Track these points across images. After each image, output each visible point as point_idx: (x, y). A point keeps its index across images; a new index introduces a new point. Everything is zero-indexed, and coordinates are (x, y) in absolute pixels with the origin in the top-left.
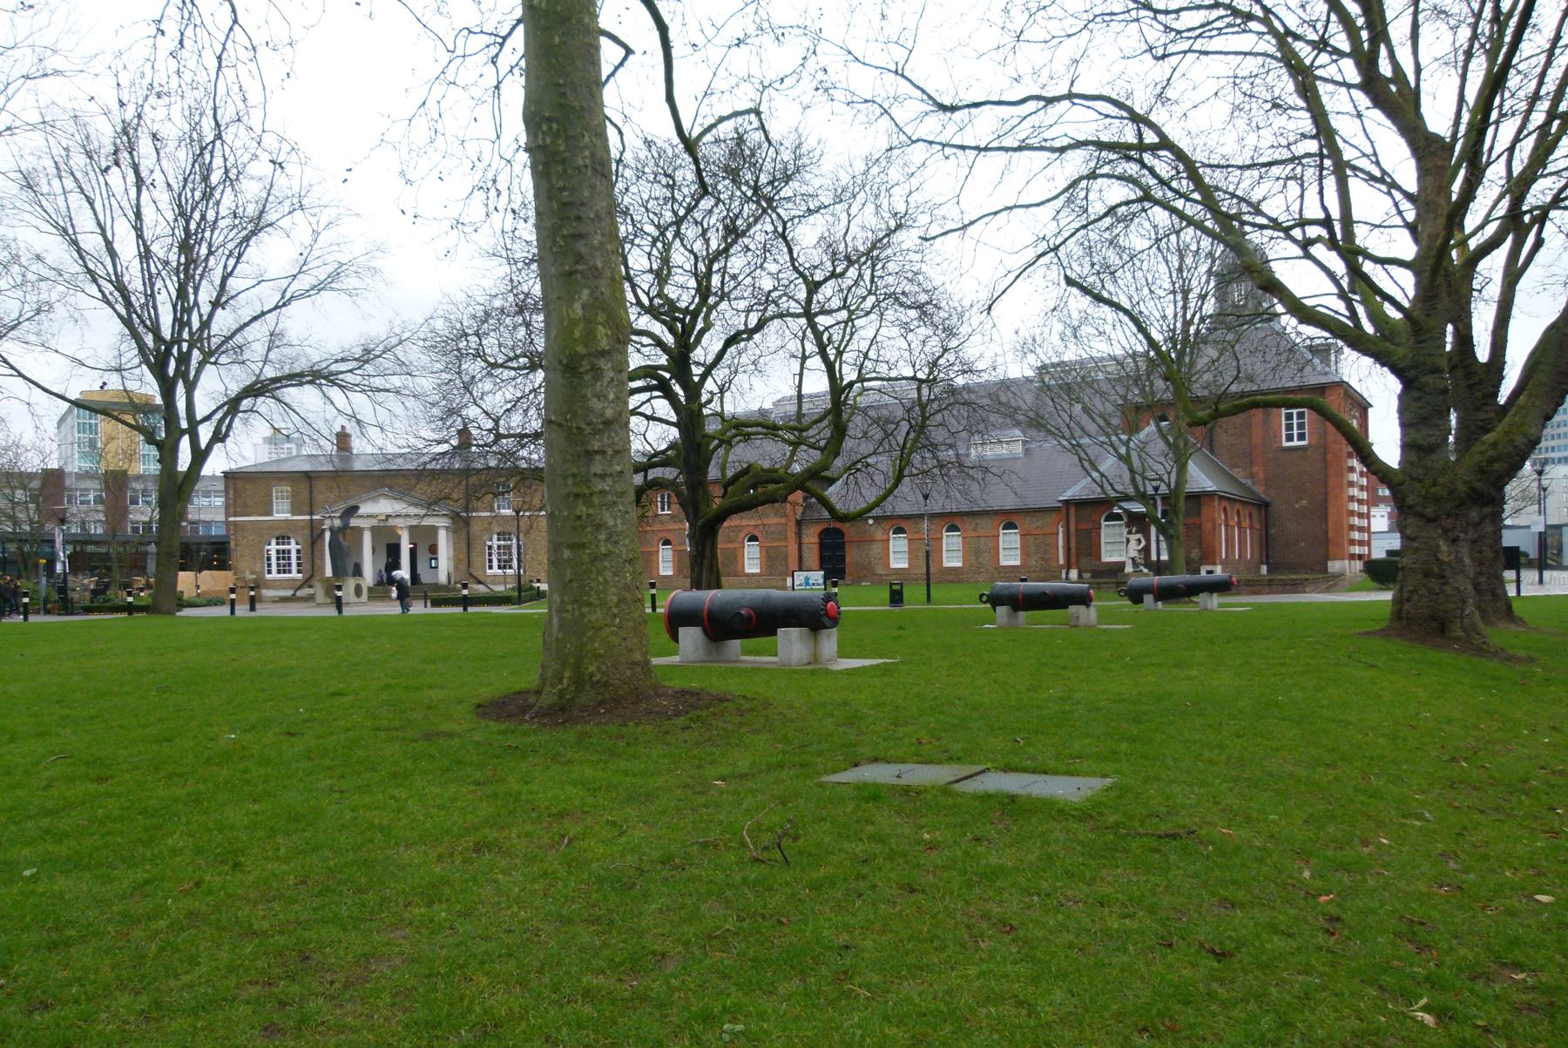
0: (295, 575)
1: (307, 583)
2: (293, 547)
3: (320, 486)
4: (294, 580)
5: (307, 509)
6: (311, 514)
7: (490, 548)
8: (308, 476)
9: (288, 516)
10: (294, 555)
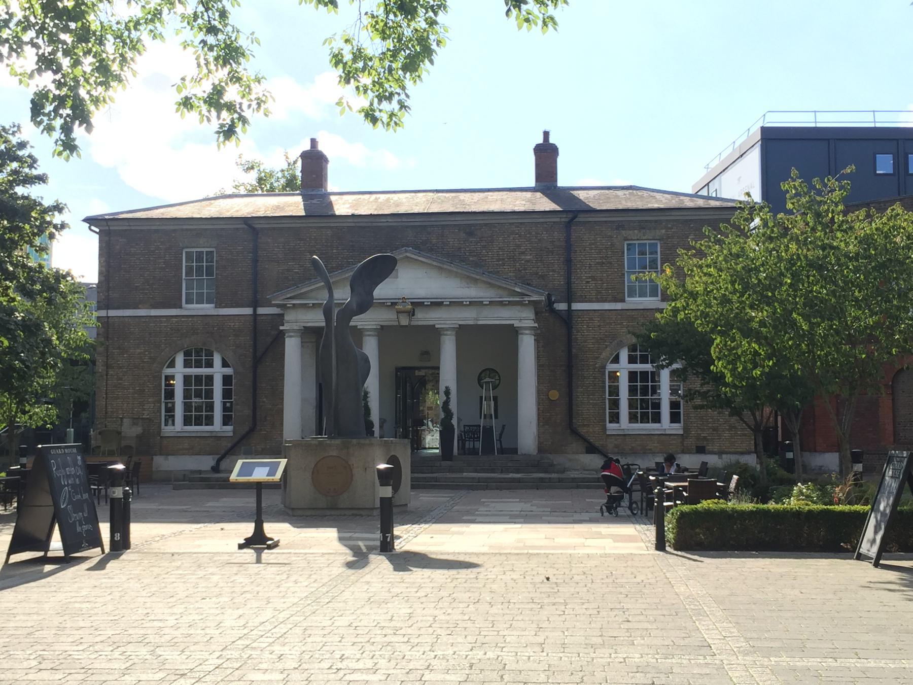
2: (218, 371)
4: (217, 438)
6: (255, 304)
7: (614, 377)
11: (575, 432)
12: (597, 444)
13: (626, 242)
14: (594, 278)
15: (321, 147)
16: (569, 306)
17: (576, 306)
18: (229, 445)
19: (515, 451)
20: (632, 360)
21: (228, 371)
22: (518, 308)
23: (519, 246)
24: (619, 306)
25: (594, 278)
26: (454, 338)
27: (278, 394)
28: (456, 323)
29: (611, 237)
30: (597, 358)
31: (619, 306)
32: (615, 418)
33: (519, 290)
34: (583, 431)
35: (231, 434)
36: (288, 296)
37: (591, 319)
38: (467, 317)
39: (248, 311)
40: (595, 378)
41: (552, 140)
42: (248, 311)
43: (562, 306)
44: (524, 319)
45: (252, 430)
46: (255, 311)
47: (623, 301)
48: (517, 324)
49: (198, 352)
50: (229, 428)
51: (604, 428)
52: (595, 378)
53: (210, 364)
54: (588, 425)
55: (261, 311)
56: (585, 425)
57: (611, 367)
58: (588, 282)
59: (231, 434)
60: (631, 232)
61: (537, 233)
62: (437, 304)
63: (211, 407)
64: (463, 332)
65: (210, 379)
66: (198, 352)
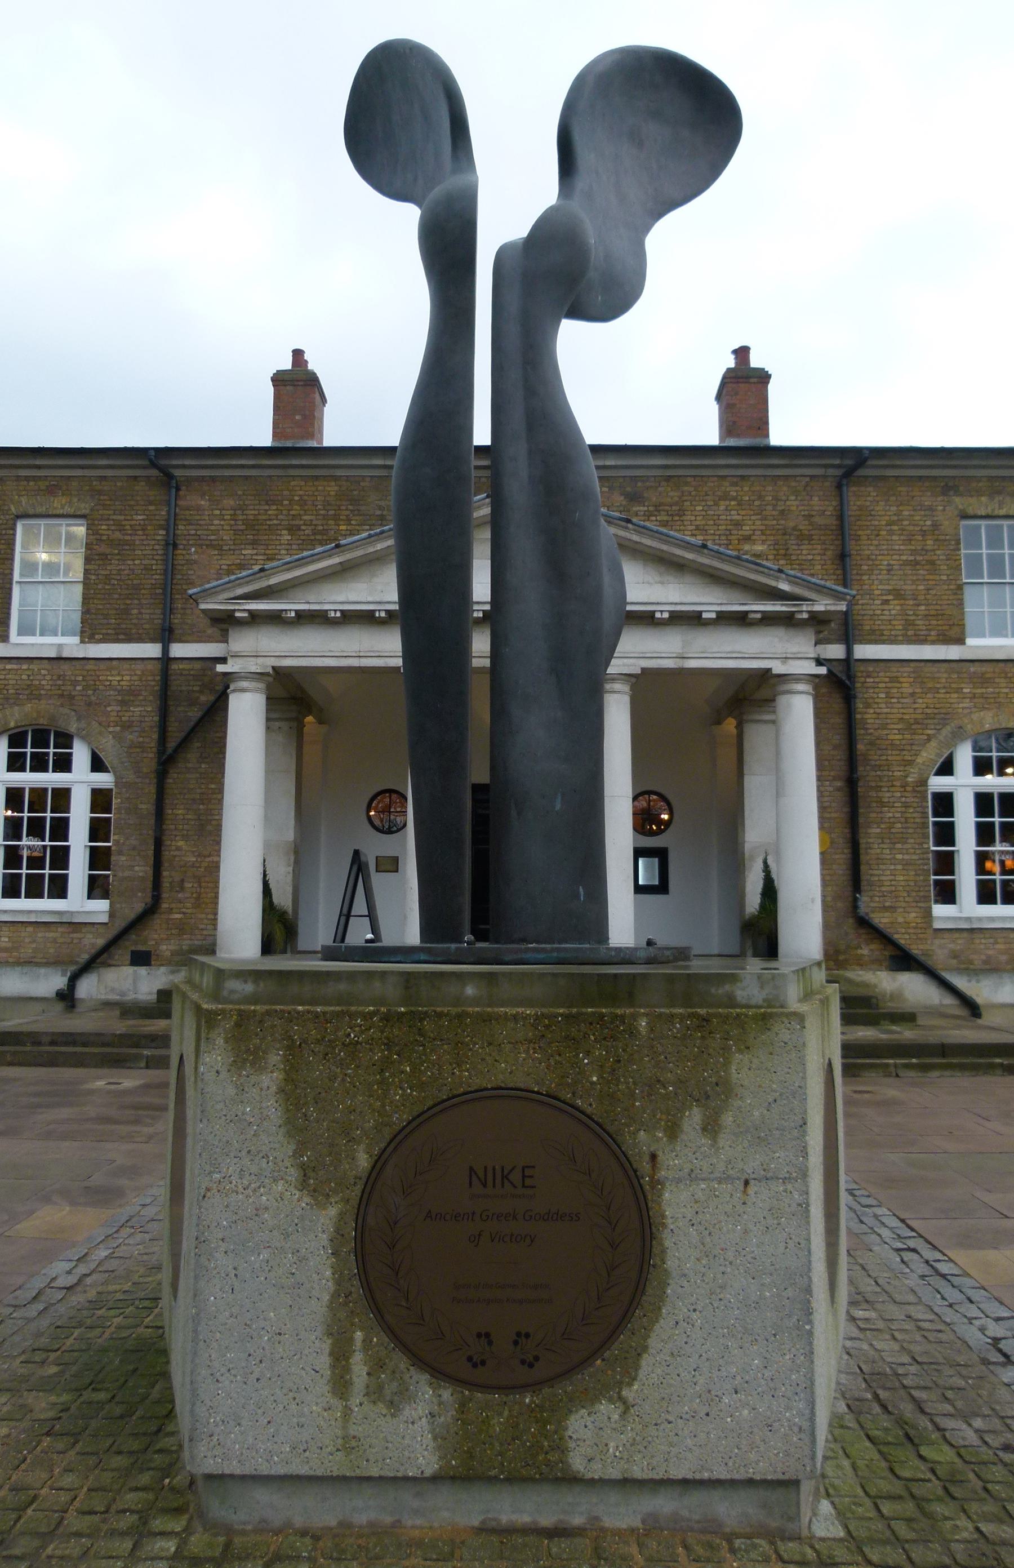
0: (78, 902)
1: (123, 943)
2: (81, 780)
3: (208, 511)
4: (74, 926)
5: (151, 615)
6: (167, 635)
7: (944, 803)
8: (163, 470)
9: (71, 645)
10: (80, 816)
13: (964, 522)
14: (898, 594)
15: (313, 365)
16: (849, 651)
17: (864, 651)
18: (101, 942)
20: (981, 767)
21: (104, 780)
23: (738, 524)
24: (952, 652)
25: (898, 594)
26: (626, 699)
27: (209, 830)
29: (931, 509)
30: (911, 763)
31: (952, 652)
32: (947, 893)
33: (784, 586)
34: (881, 920)
35: (104, 919)
36: (240, 591)
37: (894, 679)
39: (152, 650)
40: (906, 805)
41: (756, 361)
42: (152, 650)
44: (793, 655)
45: (151, 911)
46: (165, 651)
47: (960, 641)
48: (778, 668)
49: (41, 738)
50: (101, 906)
51: (928, 912)
52: (906, 805)
53: (64, 764)
54: (892, 909)
55: (179, 650)
56: (885, 909)
57: (939, 783)
58: (886, 602)
59: (104, 919)
60: (973, 500)
61: (776, 499)
63: (61, 857)
65: (62, 797)
66: (41, 738)
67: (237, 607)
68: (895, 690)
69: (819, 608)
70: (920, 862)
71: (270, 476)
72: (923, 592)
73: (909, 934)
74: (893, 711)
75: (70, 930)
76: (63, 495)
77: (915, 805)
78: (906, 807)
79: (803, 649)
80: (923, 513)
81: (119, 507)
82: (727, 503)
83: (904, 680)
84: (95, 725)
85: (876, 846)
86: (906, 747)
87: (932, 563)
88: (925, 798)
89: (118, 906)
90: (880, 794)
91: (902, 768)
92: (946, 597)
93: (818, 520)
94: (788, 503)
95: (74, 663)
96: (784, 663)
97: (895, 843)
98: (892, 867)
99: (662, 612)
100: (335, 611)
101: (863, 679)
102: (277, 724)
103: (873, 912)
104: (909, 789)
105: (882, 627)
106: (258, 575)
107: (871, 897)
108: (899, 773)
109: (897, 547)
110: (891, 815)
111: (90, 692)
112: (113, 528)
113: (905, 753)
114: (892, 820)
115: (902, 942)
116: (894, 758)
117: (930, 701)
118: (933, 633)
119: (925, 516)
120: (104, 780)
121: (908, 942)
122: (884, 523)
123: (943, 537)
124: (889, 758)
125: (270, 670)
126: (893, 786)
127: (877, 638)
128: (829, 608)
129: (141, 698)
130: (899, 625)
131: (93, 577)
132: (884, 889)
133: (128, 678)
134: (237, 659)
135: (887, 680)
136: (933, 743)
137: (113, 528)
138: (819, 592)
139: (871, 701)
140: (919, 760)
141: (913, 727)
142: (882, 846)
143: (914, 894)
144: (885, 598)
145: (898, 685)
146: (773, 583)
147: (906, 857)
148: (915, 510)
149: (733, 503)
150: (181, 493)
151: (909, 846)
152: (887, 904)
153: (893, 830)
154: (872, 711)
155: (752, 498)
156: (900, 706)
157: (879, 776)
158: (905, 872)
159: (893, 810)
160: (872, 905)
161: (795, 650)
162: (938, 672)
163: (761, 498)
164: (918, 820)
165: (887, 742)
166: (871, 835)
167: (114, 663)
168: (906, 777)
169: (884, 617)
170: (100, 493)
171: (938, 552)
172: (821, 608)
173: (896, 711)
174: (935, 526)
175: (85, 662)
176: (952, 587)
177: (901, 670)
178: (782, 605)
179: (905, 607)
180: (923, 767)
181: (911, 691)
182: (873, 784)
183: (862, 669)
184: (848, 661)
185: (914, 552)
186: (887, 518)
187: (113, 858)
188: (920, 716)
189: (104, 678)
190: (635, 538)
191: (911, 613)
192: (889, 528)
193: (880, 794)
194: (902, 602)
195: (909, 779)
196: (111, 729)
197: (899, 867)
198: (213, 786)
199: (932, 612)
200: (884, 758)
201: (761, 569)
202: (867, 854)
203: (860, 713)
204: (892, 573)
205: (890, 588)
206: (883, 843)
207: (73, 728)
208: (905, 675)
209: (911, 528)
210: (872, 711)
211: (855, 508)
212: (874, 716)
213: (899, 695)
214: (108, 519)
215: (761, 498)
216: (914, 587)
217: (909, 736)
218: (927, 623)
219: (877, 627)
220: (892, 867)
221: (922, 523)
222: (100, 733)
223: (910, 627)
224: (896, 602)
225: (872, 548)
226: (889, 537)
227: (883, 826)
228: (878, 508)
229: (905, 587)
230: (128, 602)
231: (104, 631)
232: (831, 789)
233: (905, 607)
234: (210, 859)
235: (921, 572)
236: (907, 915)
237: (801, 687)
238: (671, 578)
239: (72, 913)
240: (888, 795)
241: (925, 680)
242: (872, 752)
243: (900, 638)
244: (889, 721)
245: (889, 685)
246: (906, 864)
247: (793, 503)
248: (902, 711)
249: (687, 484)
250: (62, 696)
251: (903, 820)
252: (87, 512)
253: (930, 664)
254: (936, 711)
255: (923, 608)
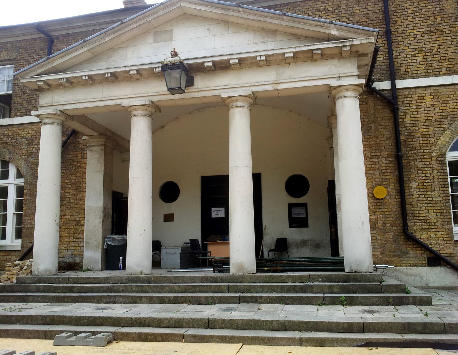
11: (410, 238)
12: (443, 253)
14: (421, 50)
16: (393, 84)
17: (401, 84)
19: (339, 264)
21: (21, 181)
22: (335, 62)
25: (421, 50)
28: (248, 91)
33: (334, 32)
34: (421, 236)
35: (19, 248)
38: (263, 81)
43: (383, 85)
48: (334, 83)
50: (19, 241)
51: (450, 232)
58: (414, 55)
59: (19, 248)
61: (347, 7)
62: (221, 66)
64: (256, 102)
67: (37, 80)
68: (422, 104)
69: (356, 42)
70: (444, 201)
71: (93, 30)
72: (436, 47)
73: (439, 244)
74: (422, 115)
75: (6, 254)
76: (5, 51)
77: (439, 168)
78: (433, 170)
79: (350, 70)
80: (434, 4)
81: (28, 54)
82: (320, 13)
83: (428, 97)
84: (16, 156)
85: (416, 193)
86: (431, 136)
87: (441, 31)
88: (444, 164)
89: (25, 242)
90: (416, 163)
91: (429, 148)
92: (451, 49)
93: (372, 15)
94: (354, 9)
95: (9, 127)
96: (338, 80)
97: (427, 191)
98: (426, 205)
99: (261, 56)
100: (85, 76)
101: (402, 100)
102: (95, 148)
103: (415, 232)
104: (434, 159)
105: (412, 69)
106: (47, 62)
107: (414, 223)
108: (427, 151)
109: (419, 25)
110: (424, 175)
111: (15, 140)
112: (25, 63)
113: (430, 139)
114: (424, 178)
115: (435, 249)
116: (424, 142)
117: (444, 108)
118: (443, 70)
119: (435, 5)
120: (21, 181)
121: (439, 249)
122: (410, 12)
123: (447, 16)
124: (421, 142)
125: (59, 112)
126: (424, 158)
127: (410, 75)
128: (363, 42)
129: (36, 141)
130: (422, 67)
131: (17, 87)
132: (421, 218)
133: (31, 132)
134: (43, 108)
135: (417, 98)
136: (447, 132)
137: (25, 63)
138: (356, 33)
139: (408, 111)
140: (440, 142)
141: (435, 124)
142: (418, 193)
143: (441, 220)
144: (413, 53)
145: (424, 101)
146: (327, 31)
147: (434, 199)
148: (429, 3)
149: (323, 12)
150: (55, 43)
151: (436, 192)
152: (424, 227)
153: (425, 184)
154: (409, 117)
155: (334, 8)
156: (426, 112)
157: (415, 153)
158: (434, 208)
159: (424, 172)
160: (415, 228)
161: (345, 72)
162: (448, 91)
163: (338, 8)
164: (440, 177)
165: (419, 134)
166: (413, 188)
167: (25, 125)
168: (432, 152)
169: (414, 64)
170: (20, 48)
171: (444, 24)
172: (359, 42)
173: (424, 115)
174: (442, 10)
175: (13, 126)
176: (454, 43)
177: (425, 92)
178: (333, 43)
179: (425, 57)
180: (442, 146)
181: (432, 103)
182: (412, 158)
183: (402, 93)
184: (393, 89)
185: (429, 26)
186: (412, 9)
187: (23, 219)
188: (438, 117)
189: (21, 133)
190: (244, 16)
191: (430, 59)
192: (413, 15)
193: (416, 163)
194: (424, 54)
195: (434, 154)
196: (23, 157)
197: (431, 205)
198: (67, 181)
199: (442, 58)
200: (418, 142)
201: (319, 23)
202: (410, 198)
203: (401, 118)
204: (417, 39)
205: (416, 47)
206: (419, 191)
207: (7, 159)
208: (427, 95)
209: (427, 13)
210: (409, 117)
211: (392, 6)
212: (410, 119)
213: (425, 106)
214: (24, 60)
215: (338, 8)
216: (431, 45)
217: (432, 129)
218: (440, 64)
219: (409, 70)
220: (426, 205)
221: (433, 10)
222: (19, 159)
223: (430, 68)
224: (420, 55)
225: (403, 27)
226: (414, 20)
227: (419, 182)
228: (405, 5)
229: (424, 46)
230: (31, 96)
231: (21, 111)
232: (387, 162)
233: (425, 57)
234: (66, 217)
235: (435, 36)
236: (437, 233)
237: (349, 93)
238: (269, 39)
239: (6, 246)
240: (421, 164)
241: (440, 97)
242: (411, 140)
243: (424, 74)
244: (419, 121)
245: (418, 101)
246: (435, 203)
247: (357, 9)
248: (426, 115)
249: (297, 6)
250: (3, 143)
251: (431, 178)
252: (15, 57)
253: (443, 88)
254: (448, 114)
255: (437, 56)
